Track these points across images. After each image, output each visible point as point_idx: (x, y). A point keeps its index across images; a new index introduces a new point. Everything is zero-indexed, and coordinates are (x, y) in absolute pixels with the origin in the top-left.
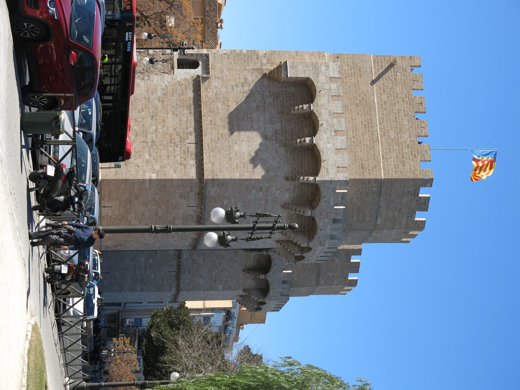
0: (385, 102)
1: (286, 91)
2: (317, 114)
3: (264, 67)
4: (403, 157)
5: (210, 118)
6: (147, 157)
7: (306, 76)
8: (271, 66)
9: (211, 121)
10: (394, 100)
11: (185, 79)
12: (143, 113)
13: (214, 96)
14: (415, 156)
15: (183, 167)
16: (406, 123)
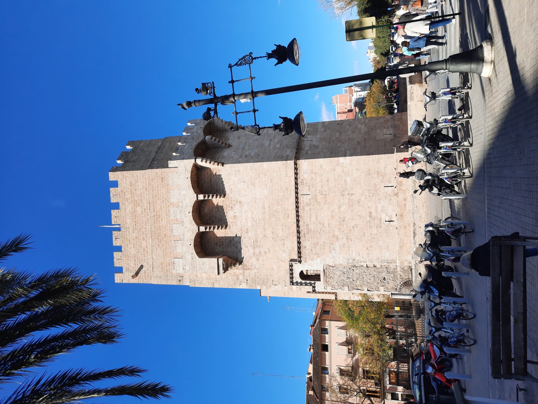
0: (144, 240)
1: (223, 248)
2: (194, 222)
3: (241, 271)
4: (131, 190)
5: (289, 220)
6: (348, 179)
7: (202, 259)
8: (235, 273)
9: (288, 217)
10: (136, 241)
11: (312, 259)
12: (353, 225)
13: (285, 242)
14: (122, 191)
15: (314, 171)
16: (128, 220)
